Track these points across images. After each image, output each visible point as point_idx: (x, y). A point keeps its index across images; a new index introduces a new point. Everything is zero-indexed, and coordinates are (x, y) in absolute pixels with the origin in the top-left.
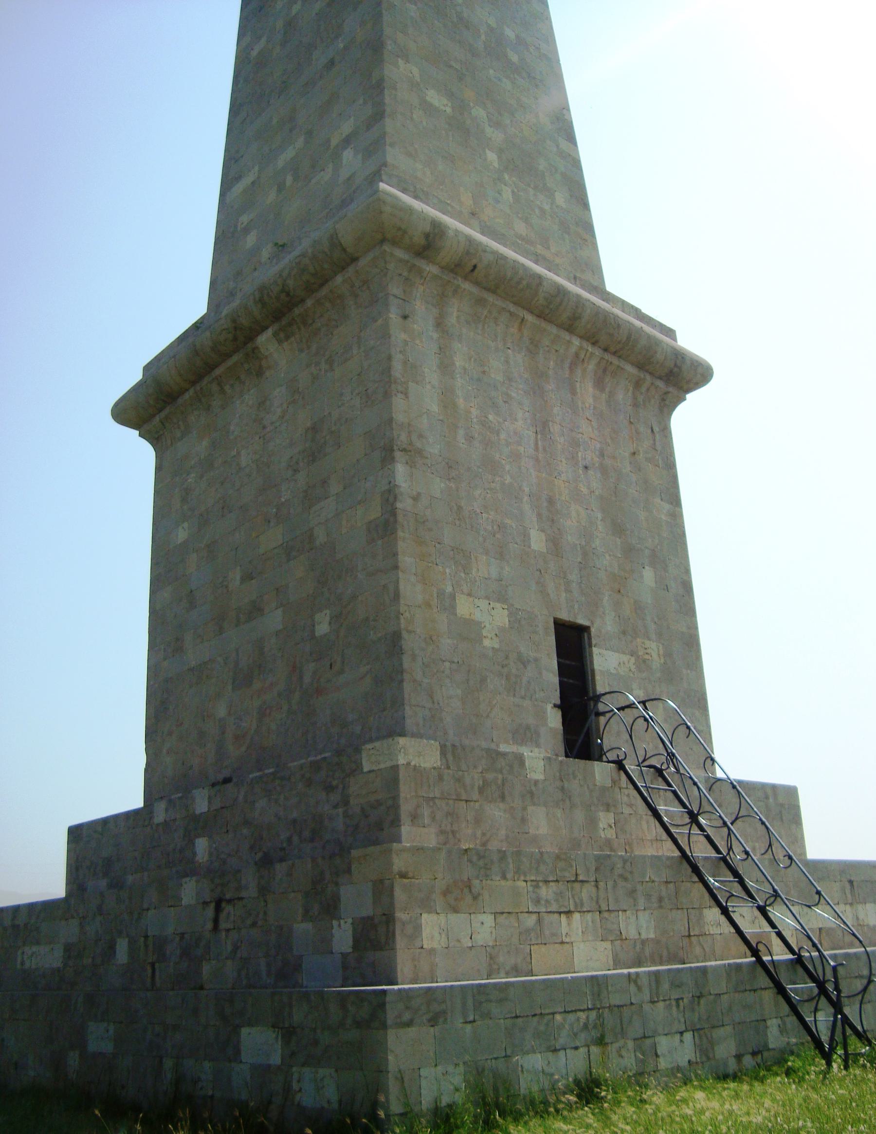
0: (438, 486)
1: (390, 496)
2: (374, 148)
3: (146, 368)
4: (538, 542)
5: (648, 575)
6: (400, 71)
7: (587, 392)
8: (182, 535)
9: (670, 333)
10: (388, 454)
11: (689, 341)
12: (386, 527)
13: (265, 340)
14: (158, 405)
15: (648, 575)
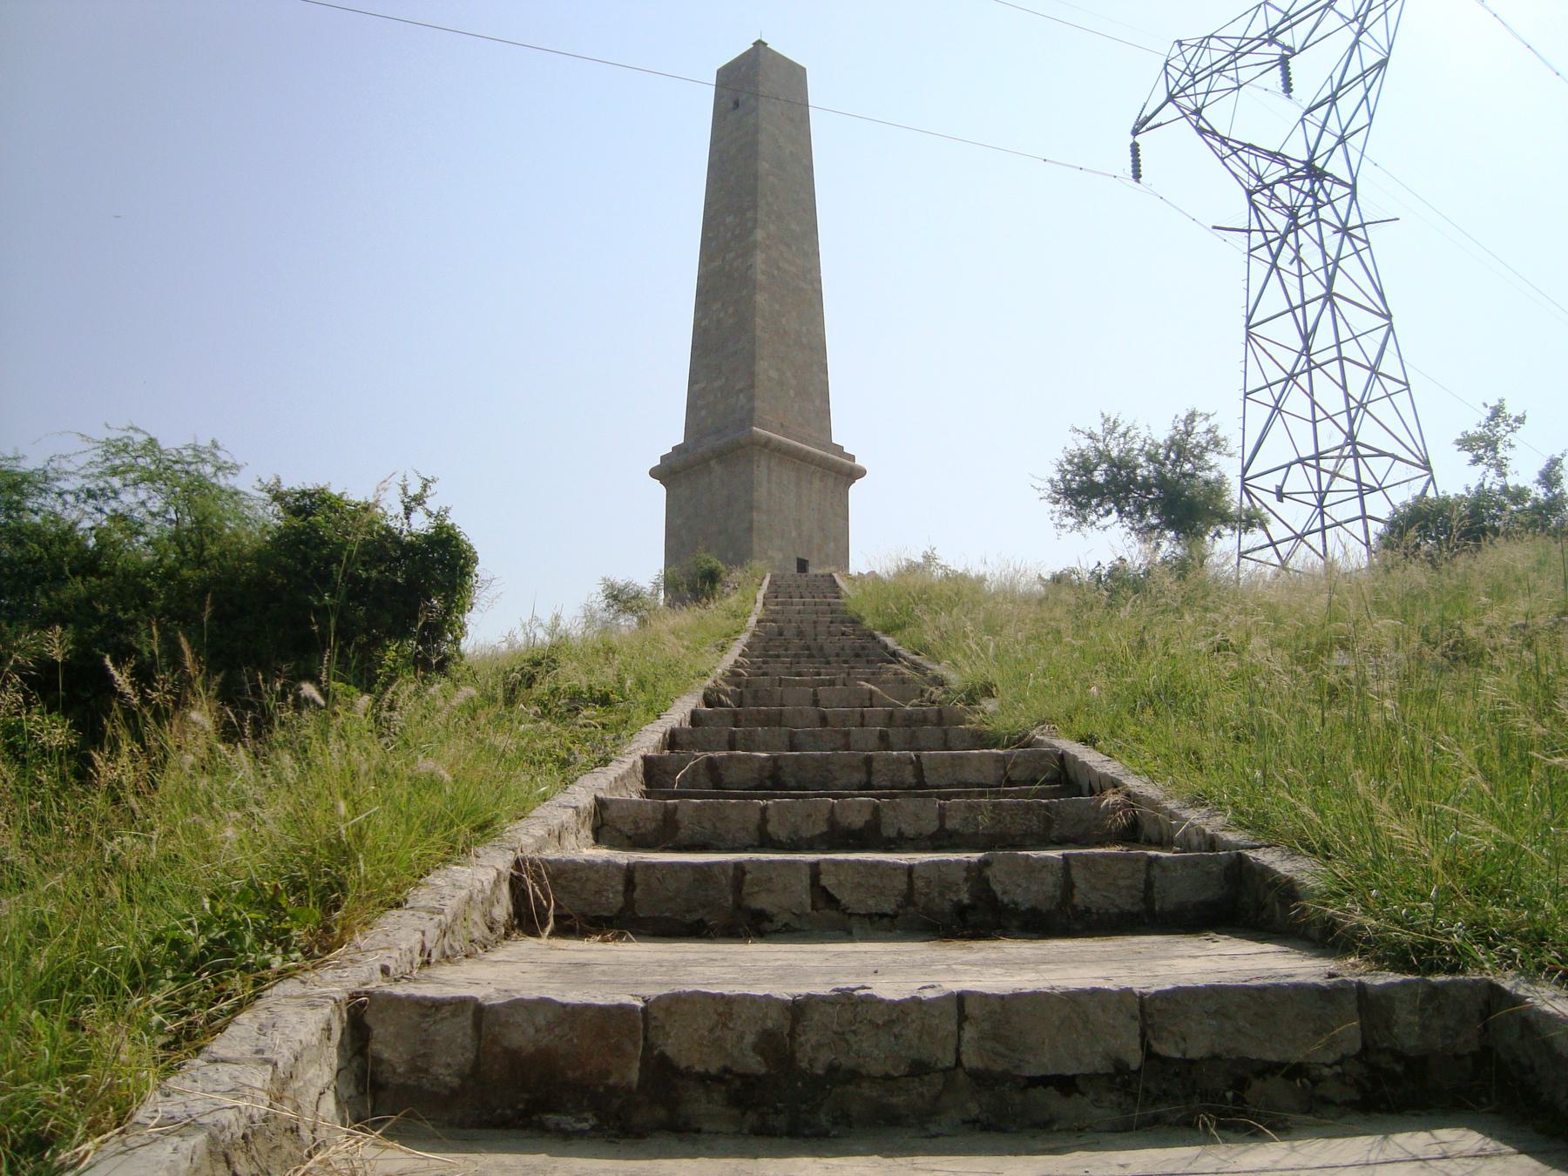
0: (765, 518)
1: (751, 522)
2: (751, 398)
3: (663, 458)
4: (794, 534)
5: (832, 545)
6: (762, 366)
7: (817, 484)
8: (679, 521)
9: (852, 458)
10: (751, 508)
11: (859, 462)
12: (750, 529)
13: (713, 463)
14: (669, 472)
15: (832, 545)
